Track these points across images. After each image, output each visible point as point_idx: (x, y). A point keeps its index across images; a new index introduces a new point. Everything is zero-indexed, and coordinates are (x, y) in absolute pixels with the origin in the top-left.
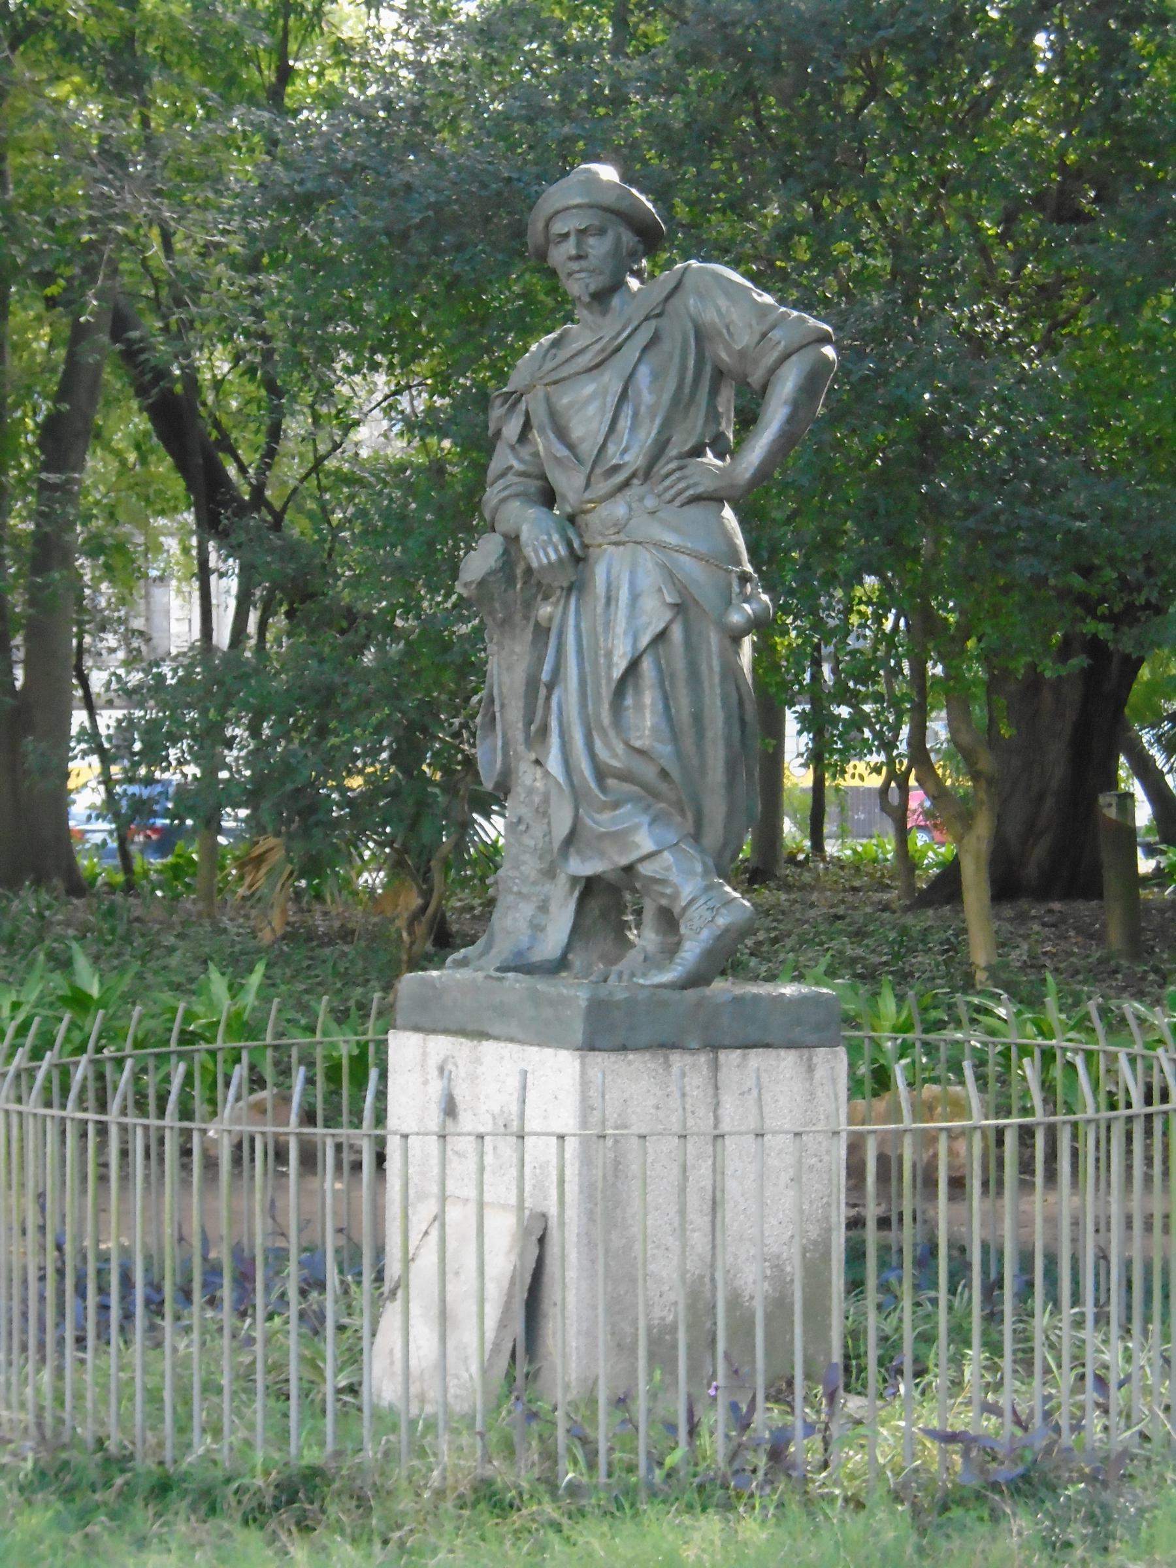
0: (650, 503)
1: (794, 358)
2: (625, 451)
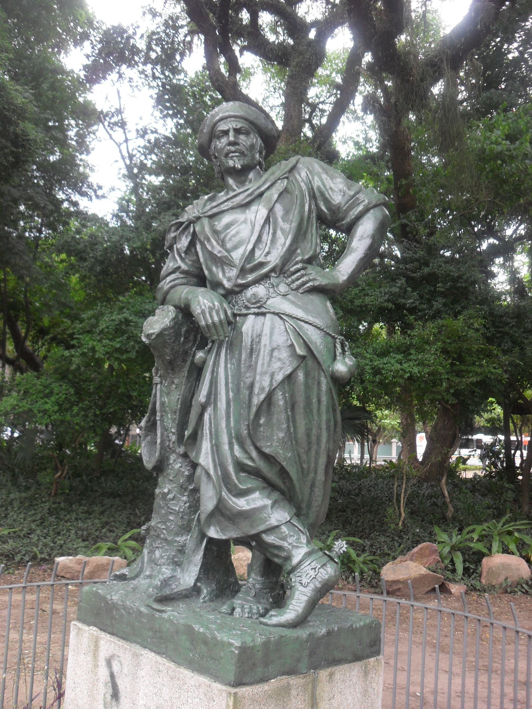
0: (283, 288)
1: (372, 211)
2: (268, 253)
